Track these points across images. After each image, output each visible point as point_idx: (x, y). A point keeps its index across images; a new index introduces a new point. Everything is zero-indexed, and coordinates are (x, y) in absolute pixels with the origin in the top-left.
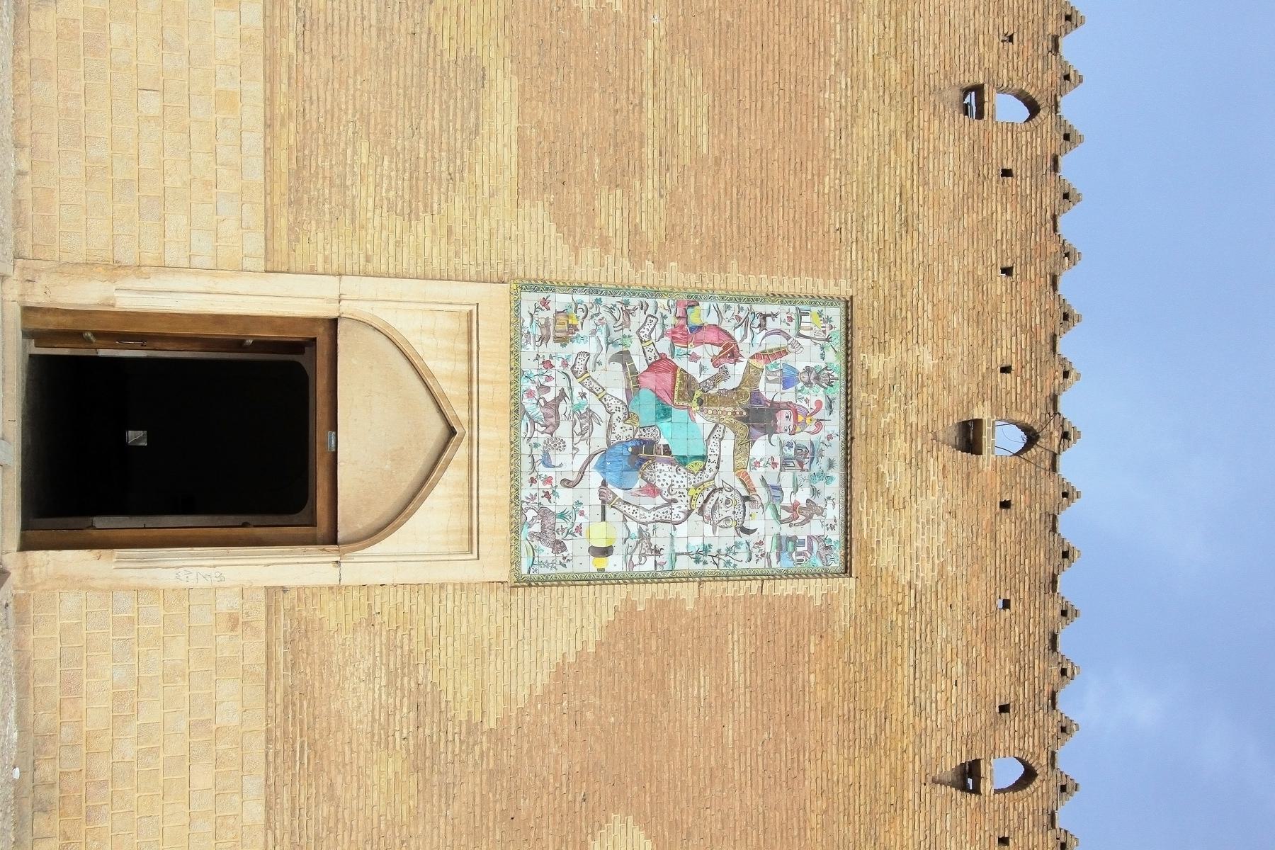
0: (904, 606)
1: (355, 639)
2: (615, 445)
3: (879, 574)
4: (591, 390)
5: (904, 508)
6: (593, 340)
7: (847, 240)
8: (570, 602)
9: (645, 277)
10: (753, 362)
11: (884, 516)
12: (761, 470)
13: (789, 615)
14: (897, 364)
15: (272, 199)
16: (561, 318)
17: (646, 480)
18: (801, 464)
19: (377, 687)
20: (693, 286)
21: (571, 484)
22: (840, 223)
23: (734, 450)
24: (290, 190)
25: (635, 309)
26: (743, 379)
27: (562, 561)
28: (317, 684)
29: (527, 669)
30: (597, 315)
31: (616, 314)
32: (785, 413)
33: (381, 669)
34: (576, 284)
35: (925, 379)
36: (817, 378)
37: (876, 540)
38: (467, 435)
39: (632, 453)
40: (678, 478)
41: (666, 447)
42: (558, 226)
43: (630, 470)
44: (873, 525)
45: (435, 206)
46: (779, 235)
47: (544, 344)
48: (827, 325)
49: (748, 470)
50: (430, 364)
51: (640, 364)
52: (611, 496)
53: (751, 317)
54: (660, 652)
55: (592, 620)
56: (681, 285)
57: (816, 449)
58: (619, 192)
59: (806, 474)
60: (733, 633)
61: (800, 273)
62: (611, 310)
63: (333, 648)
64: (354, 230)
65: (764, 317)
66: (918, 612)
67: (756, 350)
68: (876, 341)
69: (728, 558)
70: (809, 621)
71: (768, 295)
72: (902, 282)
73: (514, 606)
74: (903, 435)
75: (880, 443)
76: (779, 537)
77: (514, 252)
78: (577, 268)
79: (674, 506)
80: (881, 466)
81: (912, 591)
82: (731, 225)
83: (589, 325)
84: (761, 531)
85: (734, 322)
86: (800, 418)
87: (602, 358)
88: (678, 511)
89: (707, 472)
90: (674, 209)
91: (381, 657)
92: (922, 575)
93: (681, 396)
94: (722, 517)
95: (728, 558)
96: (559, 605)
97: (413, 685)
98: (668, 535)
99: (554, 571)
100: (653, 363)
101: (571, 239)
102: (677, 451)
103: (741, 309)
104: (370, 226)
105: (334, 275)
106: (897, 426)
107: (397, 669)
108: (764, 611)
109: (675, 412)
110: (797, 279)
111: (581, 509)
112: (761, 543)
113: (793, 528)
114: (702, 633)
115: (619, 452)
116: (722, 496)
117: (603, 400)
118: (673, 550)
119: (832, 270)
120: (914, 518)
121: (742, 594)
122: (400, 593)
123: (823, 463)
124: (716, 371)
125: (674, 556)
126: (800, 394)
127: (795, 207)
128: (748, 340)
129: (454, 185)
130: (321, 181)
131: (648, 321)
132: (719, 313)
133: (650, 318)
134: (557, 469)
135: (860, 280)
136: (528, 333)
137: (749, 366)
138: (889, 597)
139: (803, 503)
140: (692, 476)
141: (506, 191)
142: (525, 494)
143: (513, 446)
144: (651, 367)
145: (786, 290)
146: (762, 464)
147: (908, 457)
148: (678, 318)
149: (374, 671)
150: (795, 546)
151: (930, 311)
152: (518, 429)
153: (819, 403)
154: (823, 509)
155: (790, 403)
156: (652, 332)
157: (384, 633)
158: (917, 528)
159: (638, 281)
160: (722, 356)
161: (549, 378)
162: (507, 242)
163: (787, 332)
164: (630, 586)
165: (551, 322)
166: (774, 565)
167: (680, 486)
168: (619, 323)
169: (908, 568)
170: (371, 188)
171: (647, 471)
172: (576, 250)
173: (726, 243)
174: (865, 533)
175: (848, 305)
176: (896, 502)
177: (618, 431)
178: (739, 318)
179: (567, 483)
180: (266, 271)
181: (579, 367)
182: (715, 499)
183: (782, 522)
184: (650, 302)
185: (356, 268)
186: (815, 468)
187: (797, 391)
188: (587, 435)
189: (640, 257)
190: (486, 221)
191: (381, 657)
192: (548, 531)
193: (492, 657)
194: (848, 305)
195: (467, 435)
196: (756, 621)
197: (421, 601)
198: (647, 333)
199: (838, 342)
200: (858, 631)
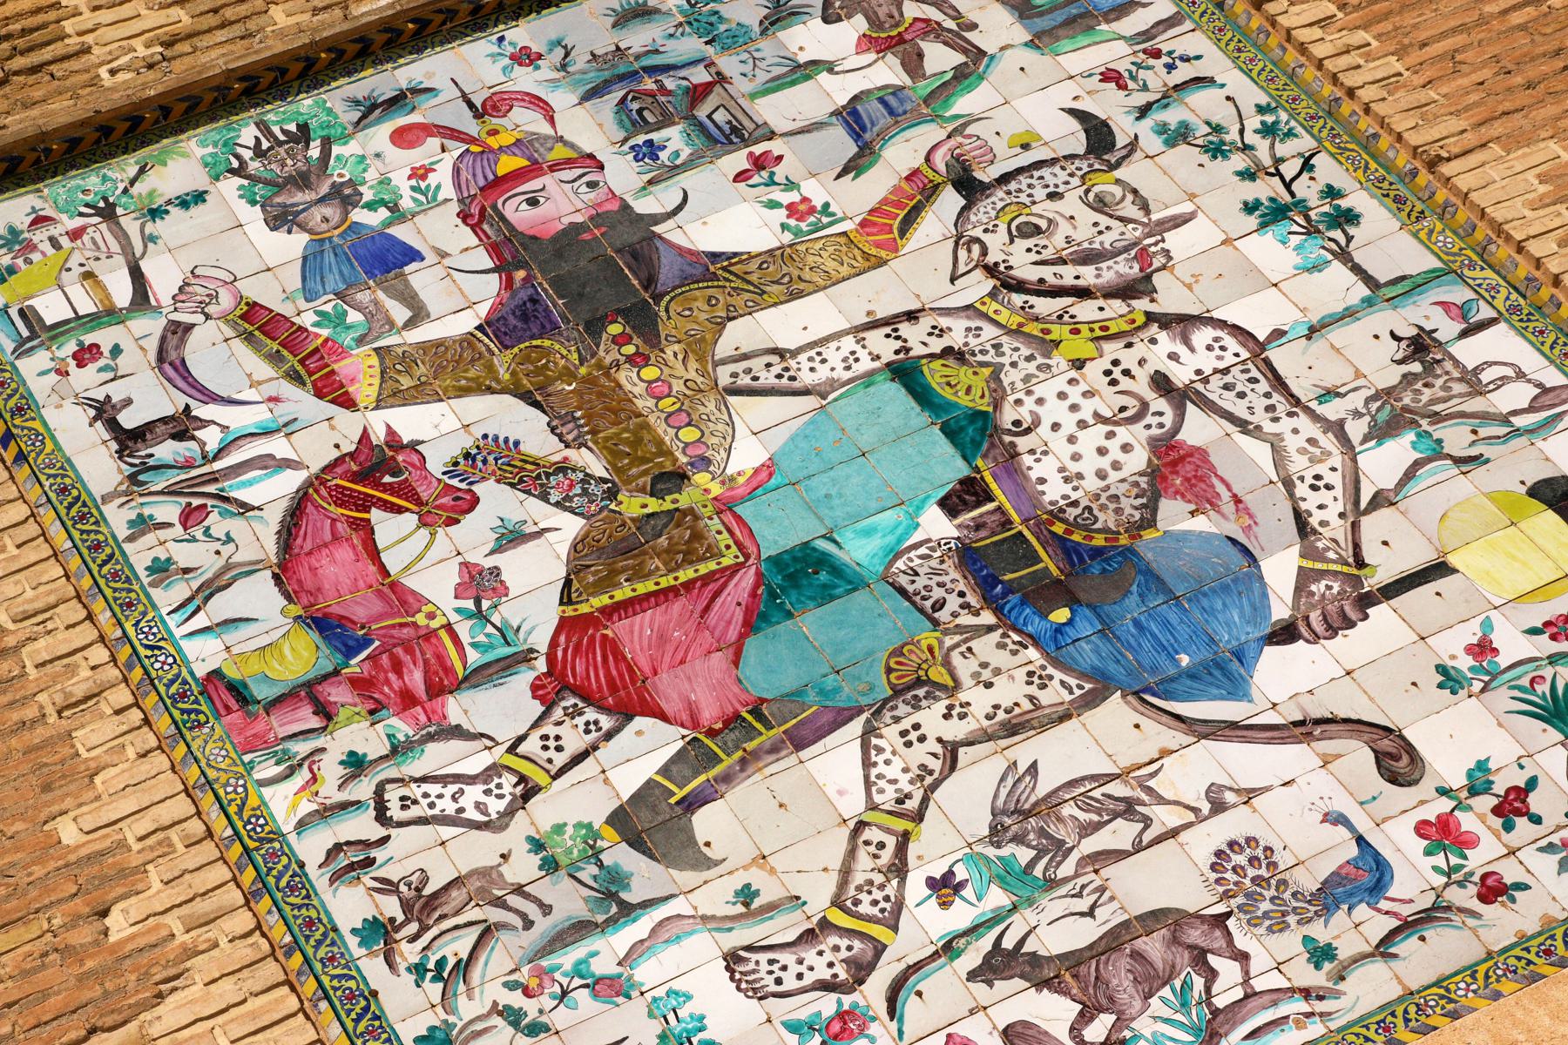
2: (1083, 676)
4: (899, 868)
6: (647, 973)
9: (202, 907)
10: (365, 389)
12: (815, 192)
17: (1151, 508)
18: (698, 94)
21: (1386, 744)
23: (794, 296)
25: (388, 886)
26: (463, 392)
36: (302, 180)
39: (1072, 601)
41: (950, 505)
48: (40, 236)
52: (1318, 588)
57: (607, 74)
59: (729, 64)
65: (128, 440)
67: (302, 402)
79: (1181, 375)
84: (1064, 95)
85: (217, 523)
86: (507, 164)
87: (716, 896)
89: (956, 339)
94: (1104, 221)
98: (1319, 344)
103: (142, 525)
111: (1465, 663)
112: (1110, 76)
113: (973, 16)
115: (1105, 648)
117: (912, 805)
118: (1368, 302)
126: (406, 203)
128: (278, 447)
131: (414, 812)
132: (211, 589)
133: (395, 812)
134: (1363, 825)
137: (390, 397)
140: (1010, 377)
153: (402, 138)
155: (464, 216)
156: (457, 778)
159: (244, 921)
160: (406, 497)
163: (152, 345)
167: (1088, 394)
168: (495, 915)
171: (1106, 519)
177: (1011, 692)
178: (189, 517)
181: (820, 962)
182: (1047, 273)
184: (311, 848)
188: (1117, 789)
189: (97, 975)
198: (474, 793)
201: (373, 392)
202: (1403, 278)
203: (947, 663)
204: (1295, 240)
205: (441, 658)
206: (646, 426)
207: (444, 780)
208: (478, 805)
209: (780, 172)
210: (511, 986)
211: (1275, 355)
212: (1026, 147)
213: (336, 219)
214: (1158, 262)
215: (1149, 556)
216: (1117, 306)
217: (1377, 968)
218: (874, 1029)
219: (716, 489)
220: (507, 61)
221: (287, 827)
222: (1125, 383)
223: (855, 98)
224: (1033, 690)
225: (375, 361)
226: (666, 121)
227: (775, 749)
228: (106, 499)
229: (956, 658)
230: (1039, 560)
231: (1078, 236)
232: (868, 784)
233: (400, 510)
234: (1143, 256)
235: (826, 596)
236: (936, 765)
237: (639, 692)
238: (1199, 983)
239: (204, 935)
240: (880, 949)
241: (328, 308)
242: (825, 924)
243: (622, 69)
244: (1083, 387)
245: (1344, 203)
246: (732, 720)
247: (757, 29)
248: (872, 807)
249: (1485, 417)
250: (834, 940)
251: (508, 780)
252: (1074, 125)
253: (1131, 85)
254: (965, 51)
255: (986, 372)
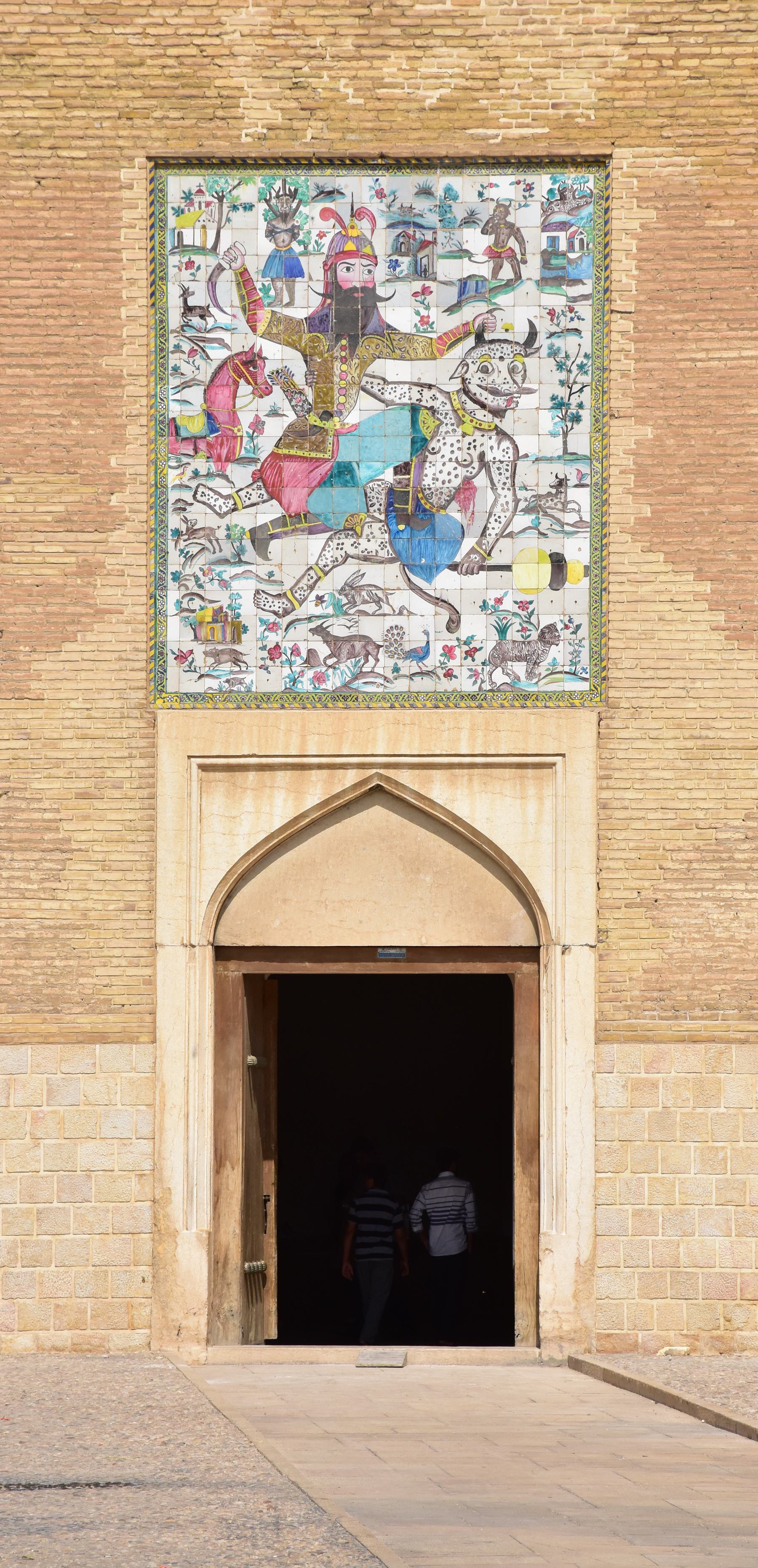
0: (664, 57)
1: (676, 926)
2: (394, 551)
3: (609, 105)
4: (312, 588)
5: (498, 58)
6: (235, 584)
7: (56, 166)
8: (634, 620)
9: (136, 507)
10: (262, 327)
11: (513, 96)
12: (434, 314)
13: (667, 264)
14: (257, 72)
15: (53, 1035)
16: (204, 632)
17: (449, 502)
18: (424, 244)
19: (748, 895)
20: (145, 430)
21: (454, 617)
22: (28, 177)
23: (402, 358)
24: (38, 1012)
25: (186, 520)
26: (288, 344)
27: (571, 630)
28: (738, 976)
29: (732, 683)
30: (197, 579)
31: (194, 550)
32: (341, 271)
33: (721, 890)
34: (152, 611)
35: (279, 21)
37: (551, 111)
38: (382, 771)
39: (407, 524)
40: (445, 451)
41: (397, 470)
42: (66, 640)
43: (433, 526)
44: (527, 116)
45: (48, 816)
46: (55, 287)
47: (244, 658)
49: (434, 336)
50: (278, 824)
51: (270, 512)
53: (190, 333)
54: (717, 480)
55: (662, 587)
56: (144, 450)
57: (401, 219)
58: (7, 547)
59: (441, 236)
60: (693, 360)
61: (115, 250)
62: (189, 558)
63: (688, 955)
64: (91, 926)
65: (188, 310)
66: (677, 28)
67: (241, 323)
68: (220, 113)
69: (574, 368)
70: (683, 229)
71: (153, 305)
72: (119, 65)
73: (635, 703)
74: (377, 63)
75: (390, 105)
76: (542, 282)
77: (109, 704)
78: (128, 611)
79: (489, 457)
80: (428, 103)
81: (641, 40)
82: (45, 367)
83: (213, 591)
84: (532, 313)
86: (350, 246)
87: (263, 570)
88: (497, 451)
89: (437, 404)
90: (28, 460)
91: (702, 889)
92: (613, 24)
93: (318, 446)
95: (574, 368)
96: (637, 636)
97: (746, 846)
98: (535, 466)
99: (586, 643)
100: (267, 491)
101: (83, 619)
102: (404, 455)
103: (178, 348)
104: (82, 905)
105: (154, 955)
106: (361, 73)
107: (722, 869)
108: (661, 307)
109: (344, 456)
110: (125, 255)
111: (491, 603)
112: (552, 313)
113: (528, 257)
114: (691, 412)
115: (406, 545)
116: (475, 379)
117: (327, 569)
118: (559, 458)
119: (107, 195)
120: (517, 40)
121: (632, 347)
122: (611, 864)
123: (422, 205)
124: (277, 389)
125: (568, 457)
126: (310, 248)
127: (8, 259)
128: (226, 336)
129: (15, 789)
130: (23, 971)
131: (204, 499)
132: (186, 385)
133: (198, 497)
134: (432, 638)
135: (121, 143)
136: (228, 681)
137: (268, 335)
138: (650, 83)
139: (489, 240)
140: (443, 429)
141: (19, 716)
142: (467, 686)
143: (397, 705)
144: (274, 494)
145: (144, 274)
146: (424, 313)
147: (413, 53)
148: (196, 452)
149: (724, 900)
150: (556, 254)
151: (165, 12)
152: (371, 696)
153: (326, 214)
154: (499, 206)
155: (325, 264)
157: (669, 886)
158: (534, 34)
159: (143, 517)
160: (253, 380)
161: (295, 651)
162: (94, 713)
163: (210, 270)
164: (613, 528)
165: (210, 648)
166: (586, 289)
167: (459, 449)
168: (208, 545)
169: (600, 49)
170: (28, 903)
171: (434, 500)
172: (100, 613)
173: (74, 376)
174: (539, 131)
175: (161, 163)
176: (488, 74)
177: (372, 546)
178: (192, 352)
179: (453, 625)
180: (154, 1041)
181: (278, 605)
183: (518, 276)
184: (173, 496)
185: (144, 924)
186: (432, 219)
187: (306, 253)
188: (380, 594)
189: (104, 513)
190: (65, 744)
191: (702, 889)
192: (525, 652)
193: (711, 734)
194: (161, 163)
195: (382, 771)
196: (676, 322)
197: (624, 835)
198: (221, 501)
199: (223, 180)
200: (703, 141)
201: (263, 329)
202: (575, 454)
203: (362, 527)
204: (557, 419)
205: (234, 448)
206: (332, 389)
207: (216, 493)
208: (220, 507)
209: (430, 299)
210: (201, 569)
211: (519, 463)
212: (507, 330)
213: (287, 242)
214: (513, 405)
215: (437, 520)
216: (490, 417)
217: (406, 681)
218: (279, 632)
219: (338, 427)
220: (373, 192)
221: (170, 486)
222: (472, 451)
223: (469, 277)
224: (379, 549)
225: (269, 316)
226: (405, 254)
227: (303, 531)
228: (173, 331)
229: (366, 527)
230: (407, 504)
231: (498, 381)
232: (320, 556)
233: (249, 383)
234: (510, 401)
235: (345, 484)
236: (340, 559)
237: (280, 490)
238: (362, 661)
239: (133, 516)
240: (294, 609)
241: (266, 284)
242: (285, 594)
243: (407, 219)
244: (460, 445)
245: (581, 412)
246: (298, 515)
247: (459, 223)
248: (317, 564)
249: (558, 520)
250: (284, 600)
251: (231, 502)
252: (527, 329)
253: (555, 321)
254: (516, 273)
255: (438, 422)
